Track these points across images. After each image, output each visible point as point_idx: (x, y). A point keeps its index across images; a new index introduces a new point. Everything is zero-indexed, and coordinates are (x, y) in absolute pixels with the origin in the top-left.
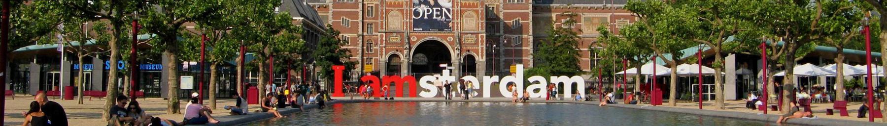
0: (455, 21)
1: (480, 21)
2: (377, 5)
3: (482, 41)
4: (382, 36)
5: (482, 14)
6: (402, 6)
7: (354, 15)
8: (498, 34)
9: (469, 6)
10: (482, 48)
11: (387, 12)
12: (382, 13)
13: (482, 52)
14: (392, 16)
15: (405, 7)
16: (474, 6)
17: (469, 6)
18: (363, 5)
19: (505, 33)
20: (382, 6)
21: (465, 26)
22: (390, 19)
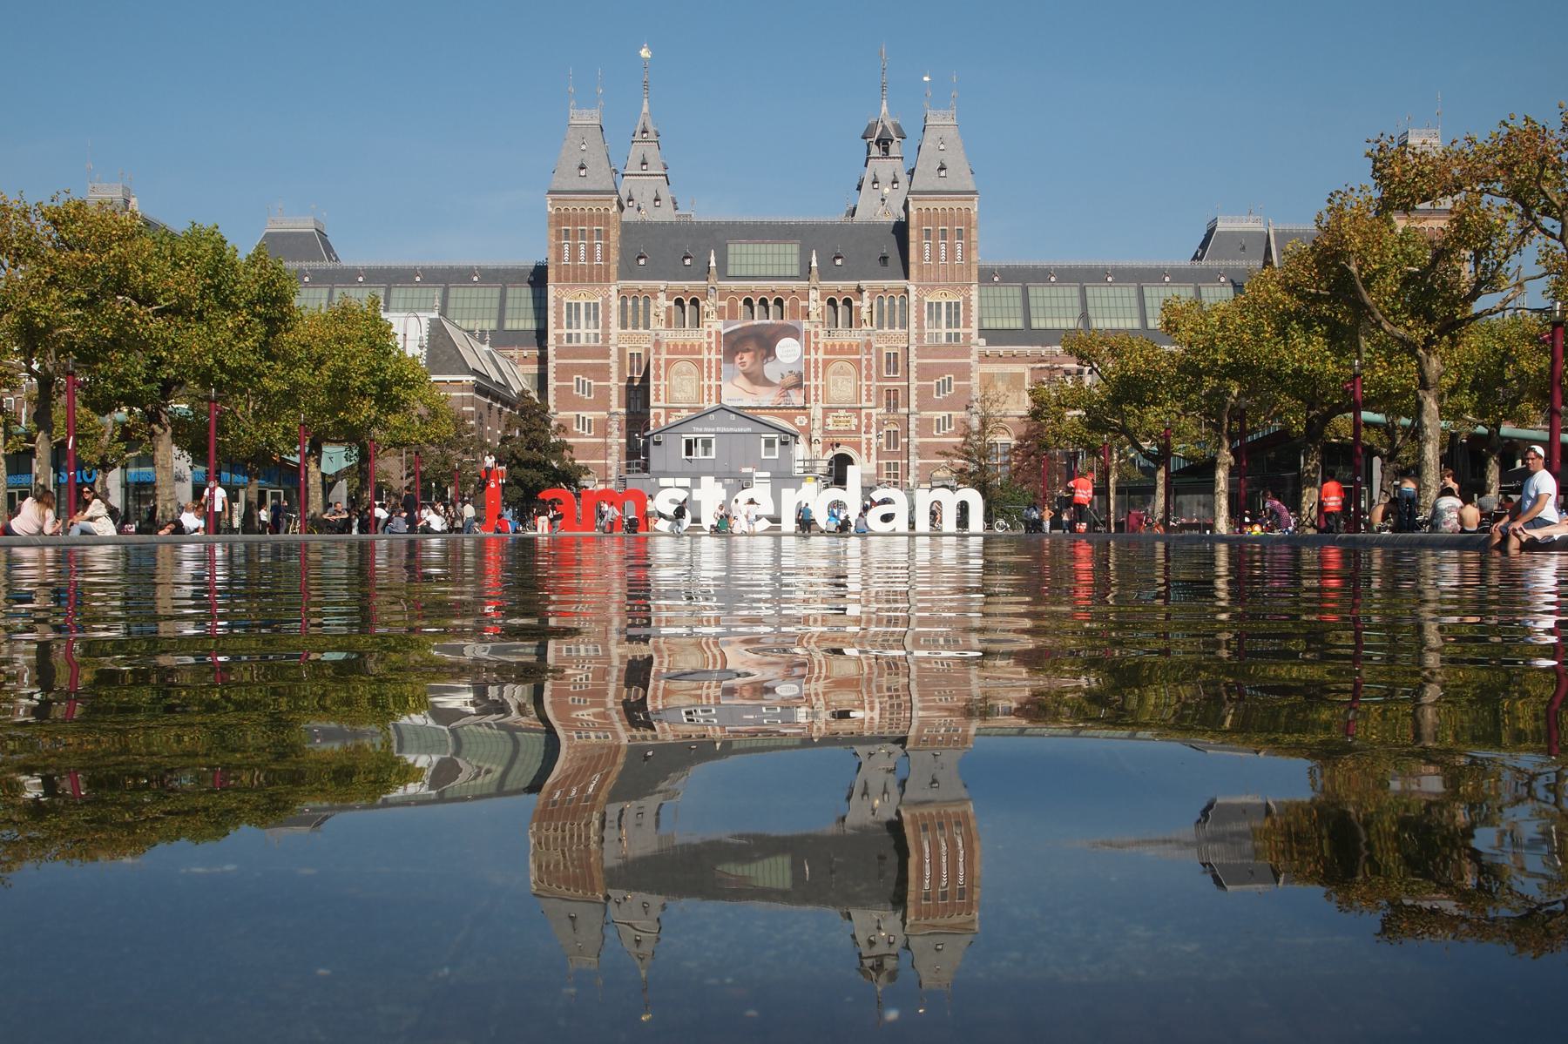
0: (813, 382)
1: (864, 382)
2: (647, 350)
3: (868, 426)
4: (658, 416)
5: (869, 367)
6: (700, 353)
7: (602, 372)
8: (905, 410)
9: (842, 351)
10: (869, 440)
11: (669, 363)
12: (658, 367)
13: (869, 449)
14: (678, 373)
15: (705, 356)
16: (852, 350)
17: (842, 351)
18: (621, 351)
19: (920, 407)
20: (657, 352)
21: (833, 393)
22: (675, 381)
